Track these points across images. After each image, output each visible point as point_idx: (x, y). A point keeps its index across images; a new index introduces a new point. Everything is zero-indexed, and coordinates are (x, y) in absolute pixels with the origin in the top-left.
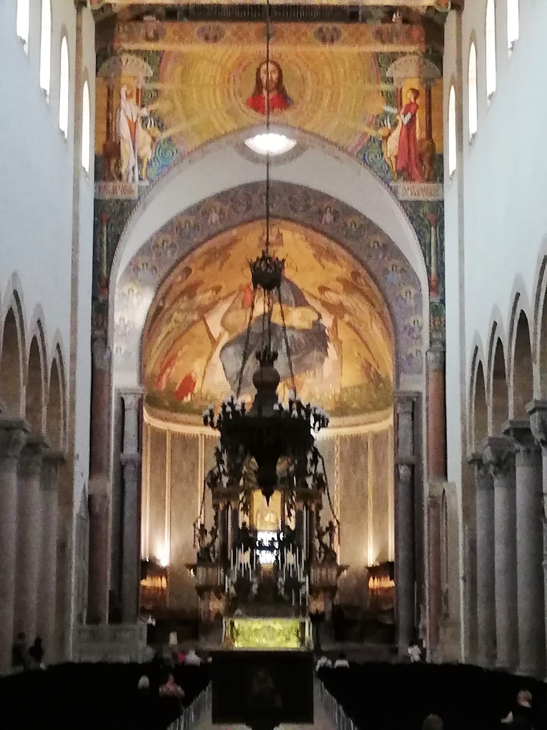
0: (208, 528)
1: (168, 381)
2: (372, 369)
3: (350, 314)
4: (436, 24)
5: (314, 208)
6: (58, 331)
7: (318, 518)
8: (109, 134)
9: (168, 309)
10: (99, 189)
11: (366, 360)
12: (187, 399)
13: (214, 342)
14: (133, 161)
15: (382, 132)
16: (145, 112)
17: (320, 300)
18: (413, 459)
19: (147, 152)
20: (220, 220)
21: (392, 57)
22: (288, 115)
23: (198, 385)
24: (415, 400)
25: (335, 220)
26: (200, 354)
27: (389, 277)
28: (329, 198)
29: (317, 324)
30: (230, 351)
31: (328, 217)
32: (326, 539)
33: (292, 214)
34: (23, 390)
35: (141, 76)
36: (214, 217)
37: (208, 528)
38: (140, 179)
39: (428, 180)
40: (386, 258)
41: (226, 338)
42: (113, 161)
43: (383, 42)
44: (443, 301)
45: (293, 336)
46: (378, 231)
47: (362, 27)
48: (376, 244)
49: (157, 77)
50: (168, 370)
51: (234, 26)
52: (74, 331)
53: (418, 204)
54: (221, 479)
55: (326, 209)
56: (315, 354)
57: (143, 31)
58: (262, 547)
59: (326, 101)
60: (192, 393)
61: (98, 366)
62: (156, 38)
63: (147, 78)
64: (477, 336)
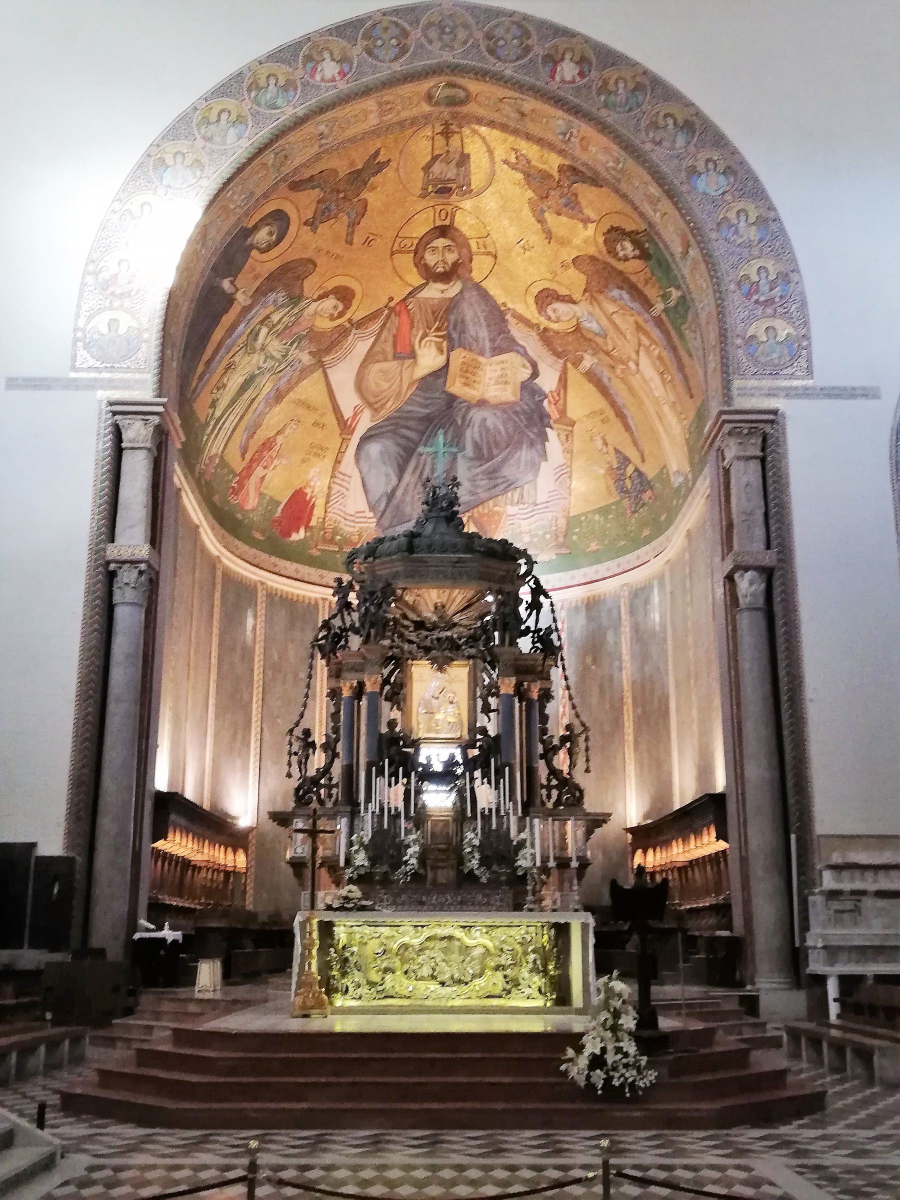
0: (319, 738)
2: (630, 470)
3: (597, 350)
5: (539, 51)
7: (544, 719)
9: (246, 310)
11: (617, 451)
12: (299, 536)
17: (538, 326)
20: (342, 74)
23: (318, 512)
24: (768, 428)
25: (581, 74)
26: (318, 450)
27: (702, 184)
29: (529, 388)
30: (374, 449)
31: (568, 70)
32: (561, 760)
33: (493, 65)
36: (329, 68)
37: (319, 738)
40: (692, 149)
41: (365, 423)
45: (484, 420)
48: (670, 121)
50: (259, 472)
54: (347, 641)
55: (564, 54)
56: (525, 454)
58: (427, 775)
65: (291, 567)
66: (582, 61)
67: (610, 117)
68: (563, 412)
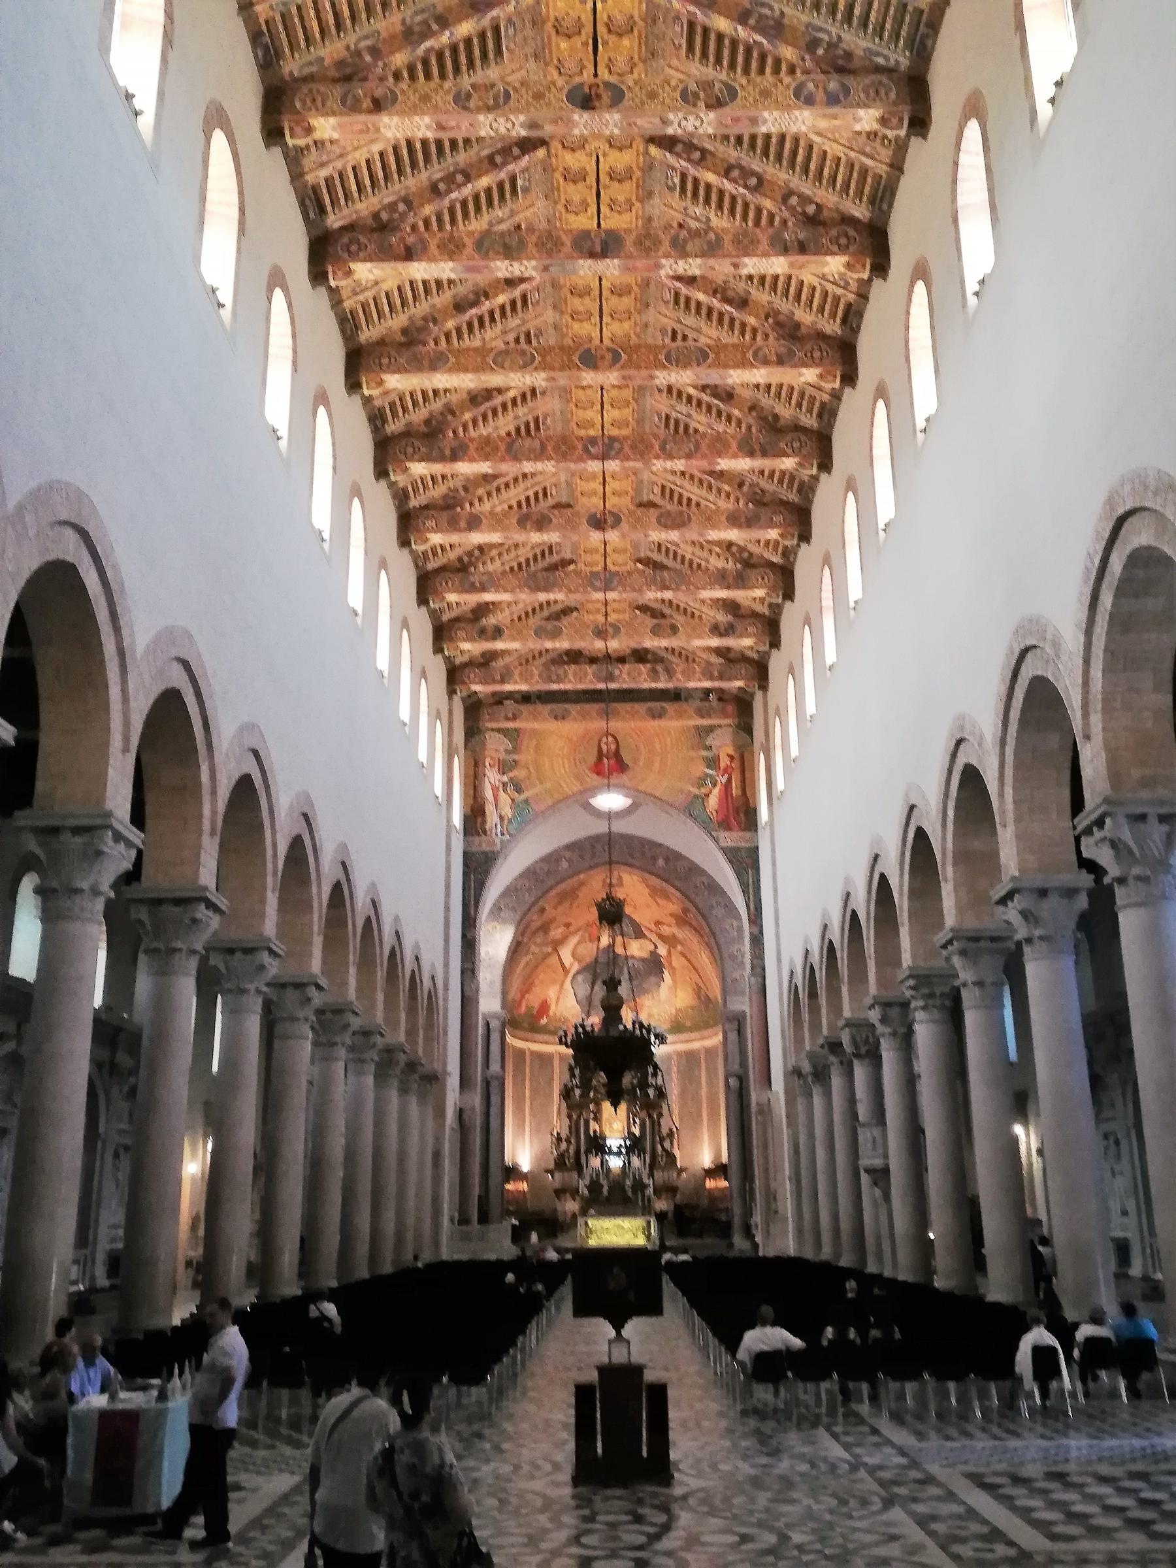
0: (564, 1136)
1: (527, 1007)
3: (682, 944)
4: (745, 700)
6: (433, 965)
7: (659, 1125)
8: (475, 797)
10: (467, 843)
12: (544, 1021)
13: (565, 970)
14: (496, 819)
15: (703, 790)
16: (505, 778)
18: (741, 1072)
19: (508, 812)
21: (710, 729)
22: (625, 778)
26: (554, 982)
27: (714, 912)
28: (659, 845)
29: (654, 955)
30: (580, 978)
31: (661, 862)
32: (667, 1145)
33: (630, 860)
34: (403, 1016)
35: (502, 749)
37: (564, 1136)
38: (502, 834)
39: (744, 830)
41: (576, 967)
42: (479, 820)
43: (703, 717)
44: (761, 932)
46: (703, 872)
47: (684, 705)
49: (516, 750)
51: (579, 707)
52: (446, 965)
53: (737, 850)
56: (653, 979)
57: (503, 714)
58: (611, 1153)
59: (657, 765)
60: (548, 1016)
61: (467, 994)
62: (515, 718)
63: (506, 751)
64: (792, 961)
65: (540, 1037)
66: (667, 860)
67: (677, 883)
68: (670, 964)
